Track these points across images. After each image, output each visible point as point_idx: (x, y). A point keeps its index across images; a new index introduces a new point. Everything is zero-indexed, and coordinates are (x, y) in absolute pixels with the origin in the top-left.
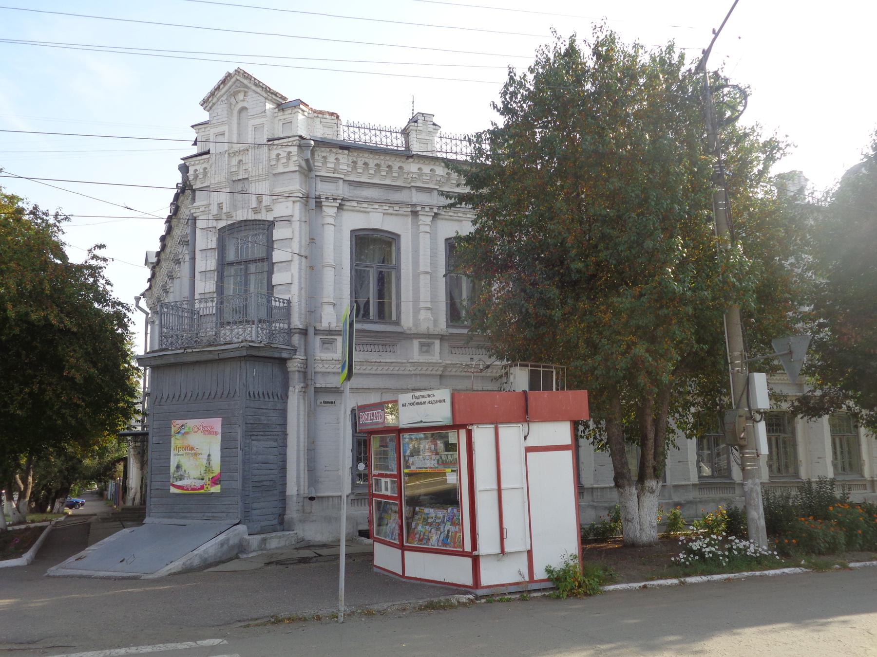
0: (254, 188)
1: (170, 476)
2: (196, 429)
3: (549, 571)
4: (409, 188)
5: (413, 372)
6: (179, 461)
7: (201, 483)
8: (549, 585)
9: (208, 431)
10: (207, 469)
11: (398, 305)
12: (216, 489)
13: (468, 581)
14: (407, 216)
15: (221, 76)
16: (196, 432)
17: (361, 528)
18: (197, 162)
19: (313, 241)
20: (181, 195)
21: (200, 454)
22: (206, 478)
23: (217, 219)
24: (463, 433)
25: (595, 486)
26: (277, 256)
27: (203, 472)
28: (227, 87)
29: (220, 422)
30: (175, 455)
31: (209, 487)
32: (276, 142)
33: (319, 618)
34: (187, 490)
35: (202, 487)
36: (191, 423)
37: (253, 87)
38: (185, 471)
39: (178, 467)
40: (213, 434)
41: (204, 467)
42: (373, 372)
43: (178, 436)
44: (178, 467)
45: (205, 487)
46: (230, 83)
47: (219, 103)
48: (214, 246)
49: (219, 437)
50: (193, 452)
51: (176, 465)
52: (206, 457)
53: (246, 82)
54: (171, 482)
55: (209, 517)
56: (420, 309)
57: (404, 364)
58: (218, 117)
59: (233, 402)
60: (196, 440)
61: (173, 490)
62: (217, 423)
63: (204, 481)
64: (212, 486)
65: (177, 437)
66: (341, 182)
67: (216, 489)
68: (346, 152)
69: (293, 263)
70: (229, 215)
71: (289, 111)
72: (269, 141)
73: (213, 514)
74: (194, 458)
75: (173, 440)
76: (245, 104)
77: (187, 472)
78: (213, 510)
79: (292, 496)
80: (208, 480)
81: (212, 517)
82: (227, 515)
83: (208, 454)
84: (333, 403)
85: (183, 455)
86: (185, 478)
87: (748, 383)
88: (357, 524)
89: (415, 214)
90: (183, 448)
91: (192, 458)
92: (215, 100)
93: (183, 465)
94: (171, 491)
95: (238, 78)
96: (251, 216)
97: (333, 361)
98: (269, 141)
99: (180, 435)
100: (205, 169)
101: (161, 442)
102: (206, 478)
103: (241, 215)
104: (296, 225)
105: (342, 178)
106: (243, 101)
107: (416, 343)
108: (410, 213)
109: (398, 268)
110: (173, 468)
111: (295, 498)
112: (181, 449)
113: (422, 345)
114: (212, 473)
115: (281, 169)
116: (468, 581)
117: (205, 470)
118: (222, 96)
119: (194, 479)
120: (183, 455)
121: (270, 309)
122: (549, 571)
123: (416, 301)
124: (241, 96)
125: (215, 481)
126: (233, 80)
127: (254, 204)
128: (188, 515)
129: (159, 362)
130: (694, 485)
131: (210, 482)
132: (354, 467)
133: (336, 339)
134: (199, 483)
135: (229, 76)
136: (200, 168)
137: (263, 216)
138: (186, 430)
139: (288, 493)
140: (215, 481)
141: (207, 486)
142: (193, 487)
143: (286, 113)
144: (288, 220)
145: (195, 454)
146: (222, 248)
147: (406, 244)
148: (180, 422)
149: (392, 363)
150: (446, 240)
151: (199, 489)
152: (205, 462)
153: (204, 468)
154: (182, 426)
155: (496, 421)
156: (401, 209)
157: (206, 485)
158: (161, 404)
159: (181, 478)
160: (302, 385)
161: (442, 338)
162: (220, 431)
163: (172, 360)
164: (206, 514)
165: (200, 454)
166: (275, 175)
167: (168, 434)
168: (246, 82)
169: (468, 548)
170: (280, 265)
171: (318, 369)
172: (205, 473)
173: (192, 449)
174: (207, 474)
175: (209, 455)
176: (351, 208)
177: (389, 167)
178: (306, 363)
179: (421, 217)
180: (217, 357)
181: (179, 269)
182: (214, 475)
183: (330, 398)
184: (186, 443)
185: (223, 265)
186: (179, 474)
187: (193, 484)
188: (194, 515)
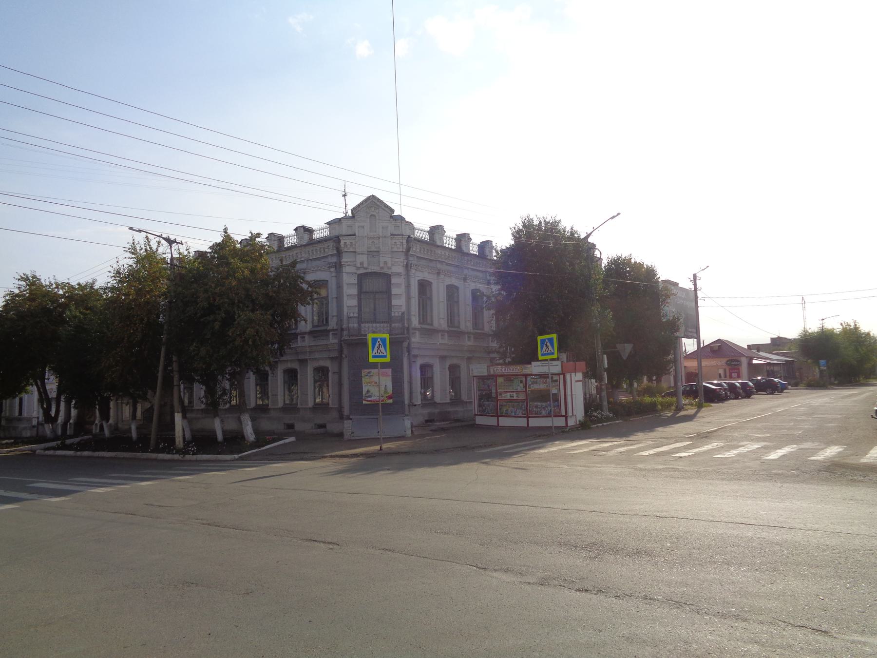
3: (580, 421)
8: (579, 426)
11: (432, 317)
12: (391, 401)
13: (564, 425)
17: (426, 419)
19: (408, 286)
23: (358, 268)
24: (562, 377)
25: (467, 401)
26: (394, 291)
28: (367, 204)
30: (365, 386)
32: (395, 236)
33: (485, 446)
34: (374, 402)
37: (383, 207)
43: (367, 377)
44: (368, 391)
46: (369, 202)
49: (391, 377)
53: (378, 203)
54: (364, 398)
56: (440, 318)
61: (364, 402)
66: (415, 257)
67: (391, 401)
68: (419, 243)
76: (375, 213)
84: (415, 362)
87: (603, 357)
89: (438, 274)
92: (359, 209)
94: (364, 403)
100: (351, 243)
103: (375, 269)
104: (403, 277)
105: (415, 255)
109: (431, 299)
110: (364, 392)
113: (442, 335)
115: (395, 249)
116: (564, 425)
118: (363, 208)
122: (580, 421)
124: (373, 209)
125: (390, 397)
126: (370, 201)
130: (449, 403)
135: (369, 198)
136: (348, 242)
137: (386, 271)
138: (371, 374)
140: (390, 397)
143: (397, 221)
144: (399, 274)
146: (360, 285)
147: (434, 286)
148: (367, 371)
150: (418, 281)
155: (571, 373)
159: (370, 396)
160: (408, 353)
161: (448, 332)
162: (391, 375)
166: (392, 252)
168: (378, 203)
169: (563, 413)
171: (412, 346)
177: (424, 249)
178: (409, 344)
185: (361, 292)
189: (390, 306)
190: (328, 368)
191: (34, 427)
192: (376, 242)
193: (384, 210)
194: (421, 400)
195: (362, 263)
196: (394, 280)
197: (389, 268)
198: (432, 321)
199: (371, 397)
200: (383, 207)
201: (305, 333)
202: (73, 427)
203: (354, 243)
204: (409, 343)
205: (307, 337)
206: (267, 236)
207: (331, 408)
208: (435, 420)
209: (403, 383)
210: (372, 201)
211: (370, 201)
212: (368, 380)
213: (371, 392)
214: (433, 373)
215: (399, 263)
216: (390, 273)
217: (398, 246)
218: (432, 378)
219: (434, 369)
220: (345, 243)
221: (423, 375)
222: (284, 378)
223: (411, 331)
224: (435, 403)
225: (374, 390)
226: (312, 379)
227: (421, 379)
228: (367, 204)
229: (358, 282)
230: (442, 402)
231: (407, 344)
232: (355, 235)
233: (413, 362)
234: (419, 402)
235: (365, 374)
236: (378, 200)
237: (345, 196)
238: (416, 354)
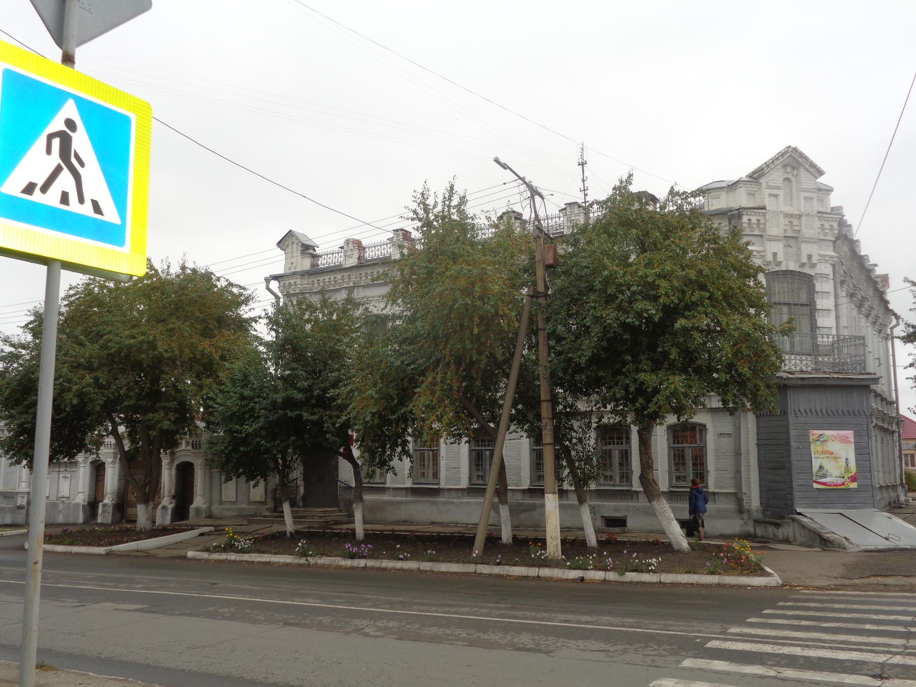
0: (806, 249)
2: (834, 439)
7: (842, 480)
9: (844, 440)
12: (854, 485)
15: (781, 147)
16: (833, 441)
18: (753, 214)
21: (839, 458)
22: (846, 477)
27: (843, 472)
29: (853, 434)
31: (849, 483)
32: (824, 215)
34: (830, 485)
35: (843, 484)
36: (828, 433)
38: (827, 471)
39: (821, 468)
43: (818, 443)
44: (821, 468)
45: (846, 483)
46: (786, 157)
47: (775, 170)
50: (833, 456)
52: (844, 460)
54: (814, 479)
58: (774, 182)
60: (835, 446)
61: (815, 486)
62: (850, 434)
67: (854, 485)
70: (779, 264)
71: (824, 192)
72: (818, 213)
76: (790, 176)
77: (829, 472)
78: (852, 502)
90: (824, 452)
93: (825, 467)
95: (793, 154)
96: (799, 269)
98: (819, 212)
99: (819, 442)
102: (846, 477)
106: (788, 173)
121: (815, 346)
125: (853, 479)
127: (804, 260)
128: (831, 505)
134: (840, 481)
136: (754, 220)
137: (806, 270)
138: (825, 438)
140: (853, 479)
142: (835, 483)
144: (825, 276)
145: (835, 458)
151: (841, 485)
152: (844, 464)
153: (843, 469)
154: (821, 435)
159: (825, 476)
162: (853, 441)
163: (817, 382)
165: (839, 458)
168: (800, 160)
170: (822, 311)
173: (832, 453)
175: (847, 459)
182: (852, 474)
184: (826, 448)
186: (822, 473)
188: (836, 505)
189: (814, 326)
191: (20, 507)
192: (795, 222)
193: (808, 171)
195: (775, 255)
196: (819, 287)
197: (813, 266)
199: (826, 477)
200: (807, 166)
202: (110, 510)
203: (762, 221)
206: (564, 206)
207: (714, 494)
210: (791, 156)
211: (788, 155)
212: (820, 449)
215: (827, 258)
217: (826, 231)
220: (749, 220)
225: (829, 465)
228: (782, 159)
232: (764, 208)
235: (815, 437)
236: (801, 155)
237: (582, 164)
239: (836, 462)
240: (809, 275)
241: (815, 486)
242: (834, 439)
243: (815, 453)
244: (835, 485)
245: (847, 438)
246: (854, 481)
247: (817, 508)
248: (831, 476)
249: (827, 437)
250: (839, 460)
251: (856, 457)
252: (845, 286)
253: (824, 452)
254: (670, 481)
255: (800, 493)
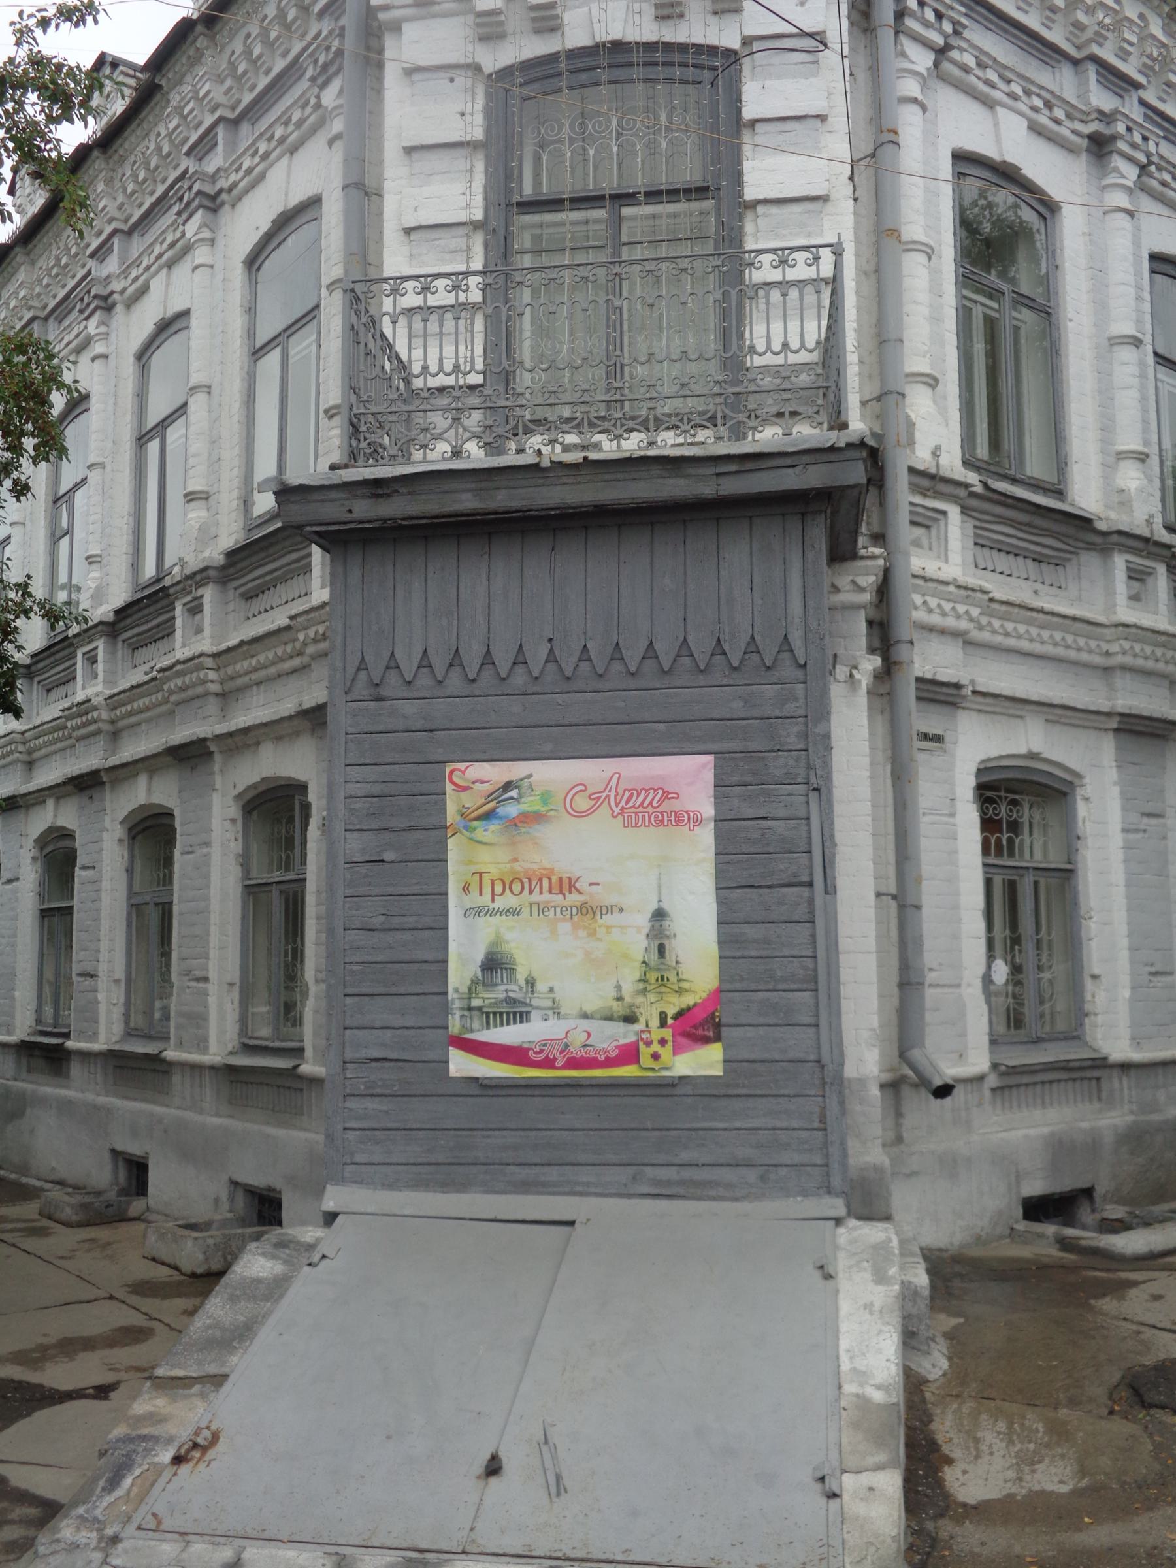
1: (446, 1009)
2: (582, 803)
4: (1076, 62)
5: (1119, 659)
6: (497, 941)
7: (625, 1034)
10: (653, 976)
14: (1070, 149)
16: (582, 815)
20: (199, 28)
21: (610, 909)
22: (649, 1015)
27: (628, 989)
29: (709, 776)
31: (666, 1053)
34: (548, 1063)
35: (629, 1054)
38: (531, 983)
40: (679, 821)
41: (637, 964)
42: (1025, 645)
43: (489, 832)
45: (645, 1052)
48: (479, 134)
49: (706, 837)
50: (573, 898)
51: (480, 956)
52: (642, 921)
55: (669, 1183)
57: (1099, 630)
59: (770, 690)
61: (461, 1064)
63: (637, 1027)
64: (676, 1051)
65: (480, 834)
69: (829, 208)
73: (687, 1174)
74: (575, 927)
75: (454, 848)
77: (541, 987)
78: (685, 1156)
79: (862, 1081)
80: (655, 1022)
81: (682, 1183)
82: (763, 1178)
83: (654, 906)
84: (938, 739)
85: (515, 912)
86: (535, 1015)
88: (1018, 1176)
91: (565, 927)
97: (951, 588)
99: (494, 826)
101: (389, 856)
102: (649, 1015)
107: (1119, 562)
108: (1085, 143)
111: (875, 1092)
112: (507, 886)
114: (680, 992)
117: (643, 980)
119: (585, 1016)
120: (515, 912)
123: (1107, 428)
128: (552, 1174)
129: (364, 509)
131: (667, 1033)
132: (987, 979)
133: (944, 513)
134: (616, 1035)
138: (530, 804)
139: (850, 1071)
141: (656, 1047)
142: (576, 1050)
145: (587, 910)
148: (492, 773)
149: (1075, 619)
151: (609, 1063)
152: (637, 944)
154: (508, 786)
156: (1067, 123)
157: (648, 1043)
158: (384, 692)
159: (517, 1013)
162: (708, 810)
164: (648, 1170)
165: (610, 909)
167: (433, 821)
170: (774, 210)
171: (920, 615)
172: (644, 991)
173: (567, 885)
174: (652, 997)
175: (660, 915)
176: (956, 72)
179: (1118, 162)
180: (708, 490)
181: (103, 329)
182: (689, 1000)
183: (929, 721)
184: (533, 860)
186: (499, 993)
187: (578, 1039)
188: (585, 1175)
190: (302, 788)
194: (993, 1042)
198: (1061, 464)
199: (521, 1016)
201: (200, 577)
204: (884, 589)
205: (209, 594)
208: (1100, 1191)
209: (830, 889)
213: (521, 977)
214: (1071, 841)
216: (732, 41)
218: (1066, 874)
219: (1082, 809)
221: (999, 852)
222: (130, 871)
223: (902, 495)
224: (1101, 1064)
226: (235, 872)
227: (988, 883)
229: (488, 131)
230: (1136, 1056)
231: (869, 580)
233: (924, 736)
234: (978, 1061)
235: (469, 800)
238: (945, 675)
239: (593, 934)
240: (713, 50)
241: (461, 1064)
242: (582, 803)
243: (466, 889)
244: (573, 1063)
245: (666, 795)
246: (706, 1040)
247: (463, 1186)
248: (555, 1009)
249: (546, 797)
250: (608, 919)
251: (720, 902)
252: (1118, 162)
253: (527, 881)
254: (243, 1020)
255: (371, 1104)
